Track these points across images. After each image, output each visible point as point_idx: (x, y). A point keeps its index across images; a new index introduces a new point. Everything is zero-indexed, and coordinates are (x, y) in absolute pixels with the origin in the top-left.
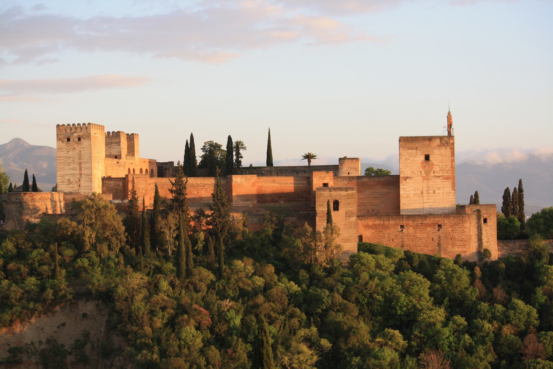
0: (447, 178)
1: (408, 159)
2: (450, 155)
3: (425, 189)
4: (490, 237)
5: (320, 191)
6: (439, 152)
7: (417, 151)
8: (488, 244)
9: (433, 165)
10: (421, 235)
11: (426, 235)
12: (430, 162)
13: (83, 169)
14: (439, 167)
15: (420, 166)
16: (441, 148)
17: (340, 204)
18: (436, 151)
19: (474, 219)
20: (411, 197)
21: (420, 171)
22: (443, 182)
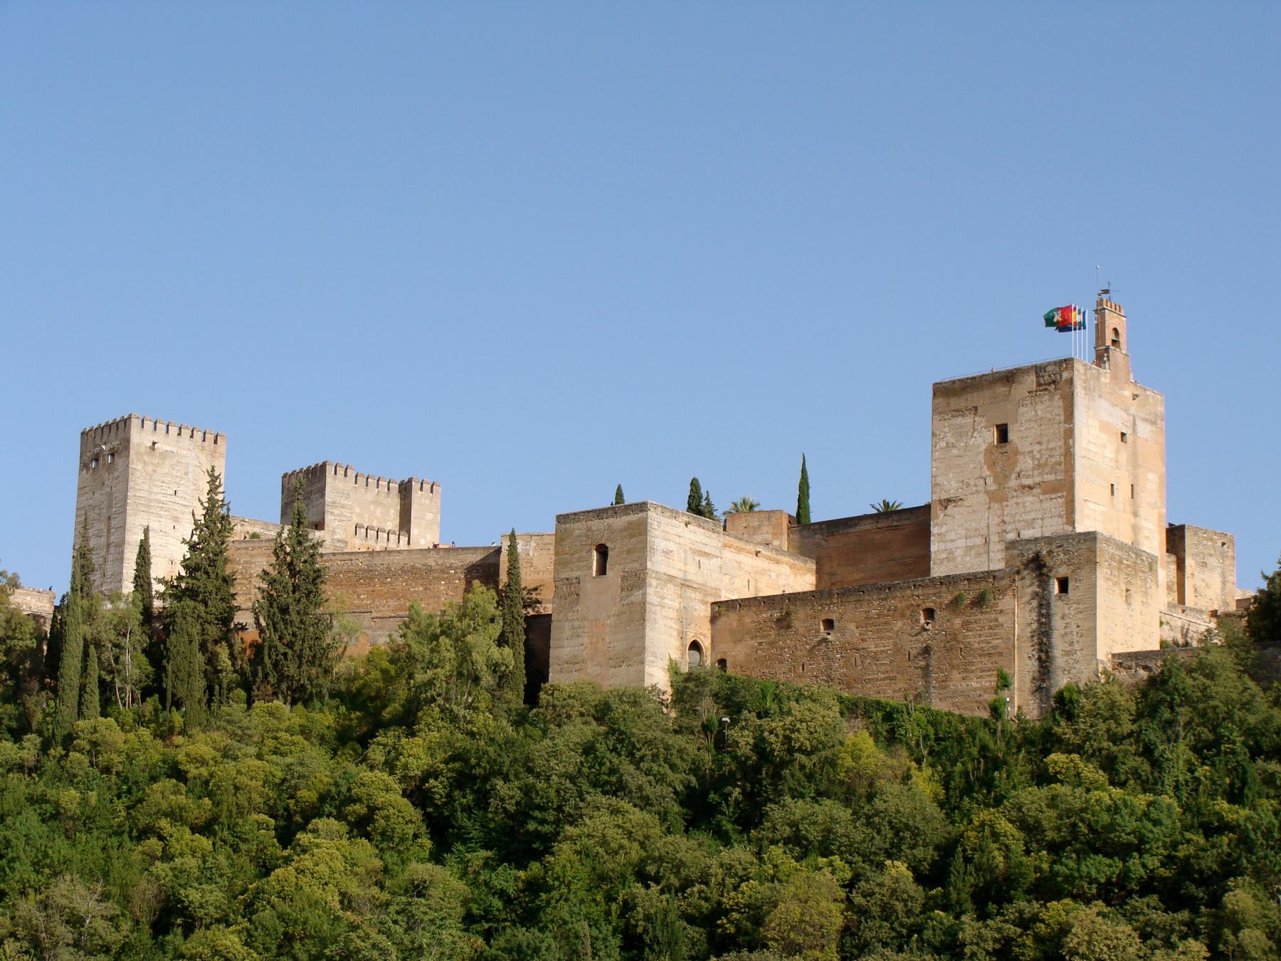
0: (1050, 489)
1: (954, 446)
2: (1062, 418)
3: (993, 529)
4: (1075, 638)
5: (564, 523)
6: (1033, 413)
7: (977, 419)
8: (1071, 661)
9: (1017, 452)
10: (876, 647)
11: (888, 645)
12: (1008, 448)
13: (112, 531)
14: (1033, 458)
15: (983, 461)
16: (1037, 399)
17: (610, 553)
18: (1024, 409)
19: (1027, 582)
20: (959, 559)
21: (981, 477)
22: (1041, 501)
